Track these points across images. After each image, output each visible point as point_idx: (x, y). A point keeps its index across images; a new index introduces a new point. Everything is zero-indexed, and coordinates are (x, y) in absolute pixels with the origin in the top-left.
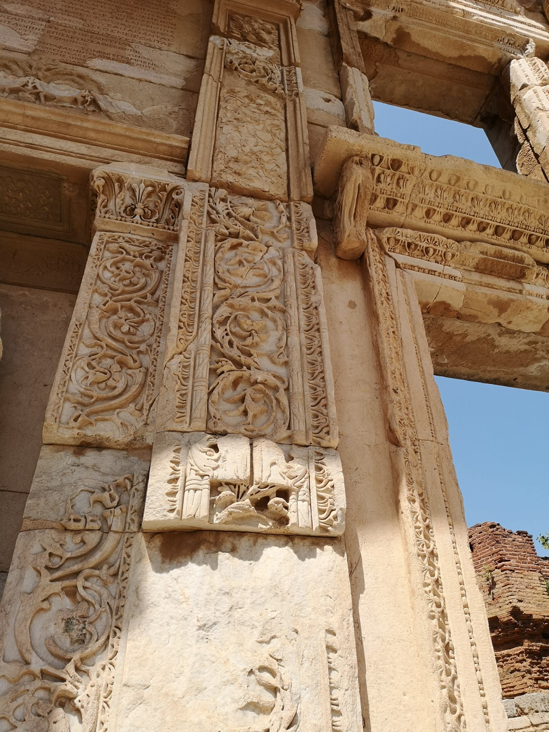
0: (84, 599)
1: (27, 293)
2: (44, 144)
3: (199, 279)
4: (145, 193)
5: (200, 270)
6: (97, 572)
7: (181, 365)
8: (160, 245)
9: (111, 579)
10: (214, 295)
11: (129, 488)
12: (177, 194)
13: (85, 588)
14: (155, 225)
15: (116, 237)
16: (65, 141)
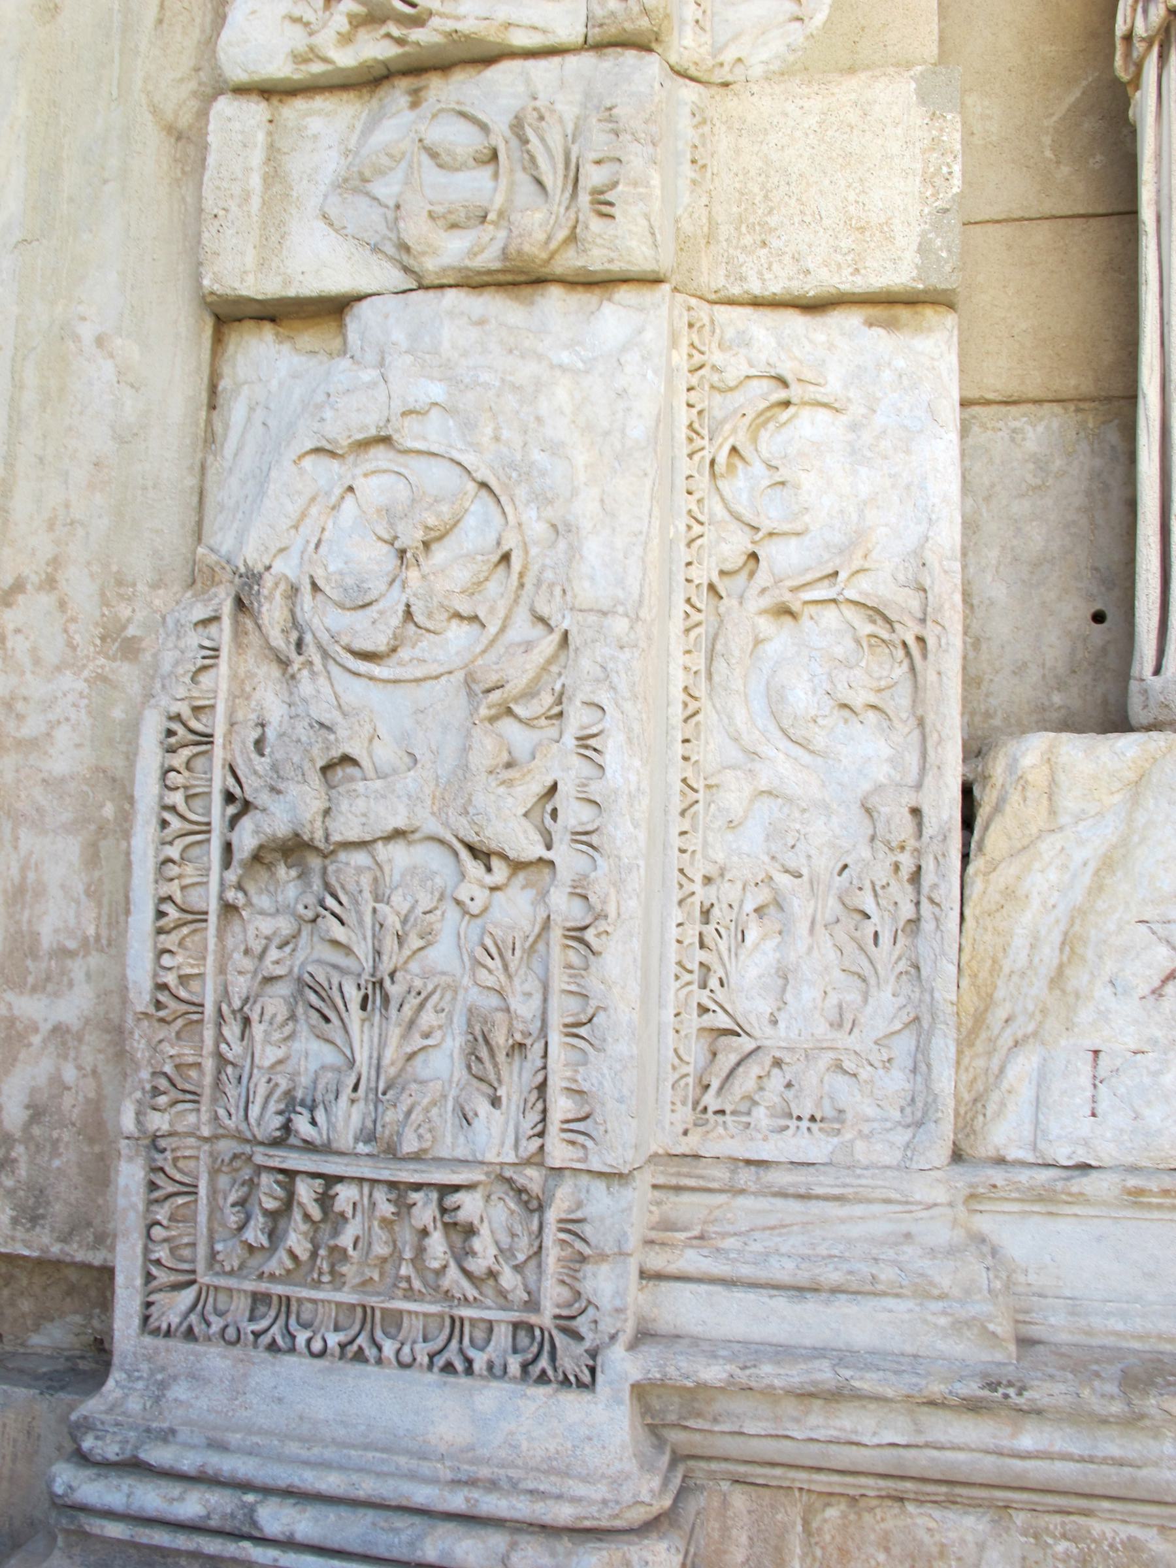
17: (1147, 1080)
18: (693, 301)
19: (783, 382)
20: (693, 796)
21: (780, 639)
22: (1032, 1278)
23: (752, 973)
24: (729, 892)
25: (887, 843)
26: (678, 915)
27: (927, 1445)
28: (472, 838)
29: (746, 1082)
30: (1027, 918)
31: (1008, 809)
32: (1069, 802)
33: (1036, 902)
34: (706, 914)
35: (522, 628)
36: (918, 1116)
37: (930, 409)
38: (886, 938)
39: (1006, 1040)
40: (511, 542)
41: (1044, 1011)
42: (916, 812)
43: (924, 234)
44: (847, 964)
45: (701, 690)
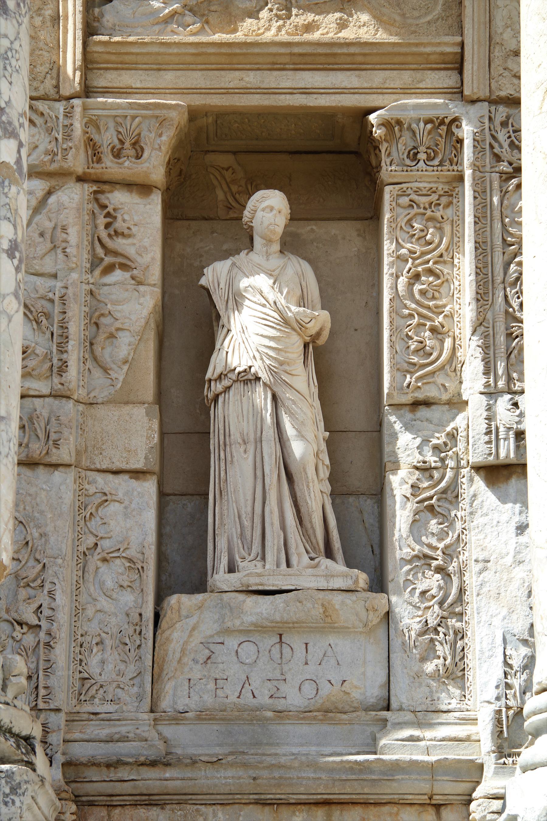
0: (439, 513)
1: (314, 227)
2: (316, 85)
3: (489, 240)
4: (425, 134)
5: (488, 229)
6: (444, 496)
7: (483, 336)
8: (446, 188)
9: (454, 500)
10: (504, 253)
11: (456, 435)
12: (457, 127)
13: (439, 506)
14: (440, 168)
15: (405, 189)
16: (334, 72)
17: (203, 687)
18: (80, 470)
19: (105, 494)
20: (78, 611)
21: (104, 568)
22: (172, 743)
23: (94, 662)
24: (89, 638)
25: (133, 623)
26: (73, 644)
27: (142, 780)
28: (18, 618)
29: (92, 692)
30: (172, 645)
31: (167, 615)
32: (184, 613)
33: (175, 641)
34: (81, 646)
35: (32, 563)
36: (140, 698)
37: (147, 504)
38: (132, 650)
39: (166, 678)
40: (29, 538)
41: (176, 670)
42: (140, 615)
43: (146, 454)
44: (121, 658)
45: (81, 582)
